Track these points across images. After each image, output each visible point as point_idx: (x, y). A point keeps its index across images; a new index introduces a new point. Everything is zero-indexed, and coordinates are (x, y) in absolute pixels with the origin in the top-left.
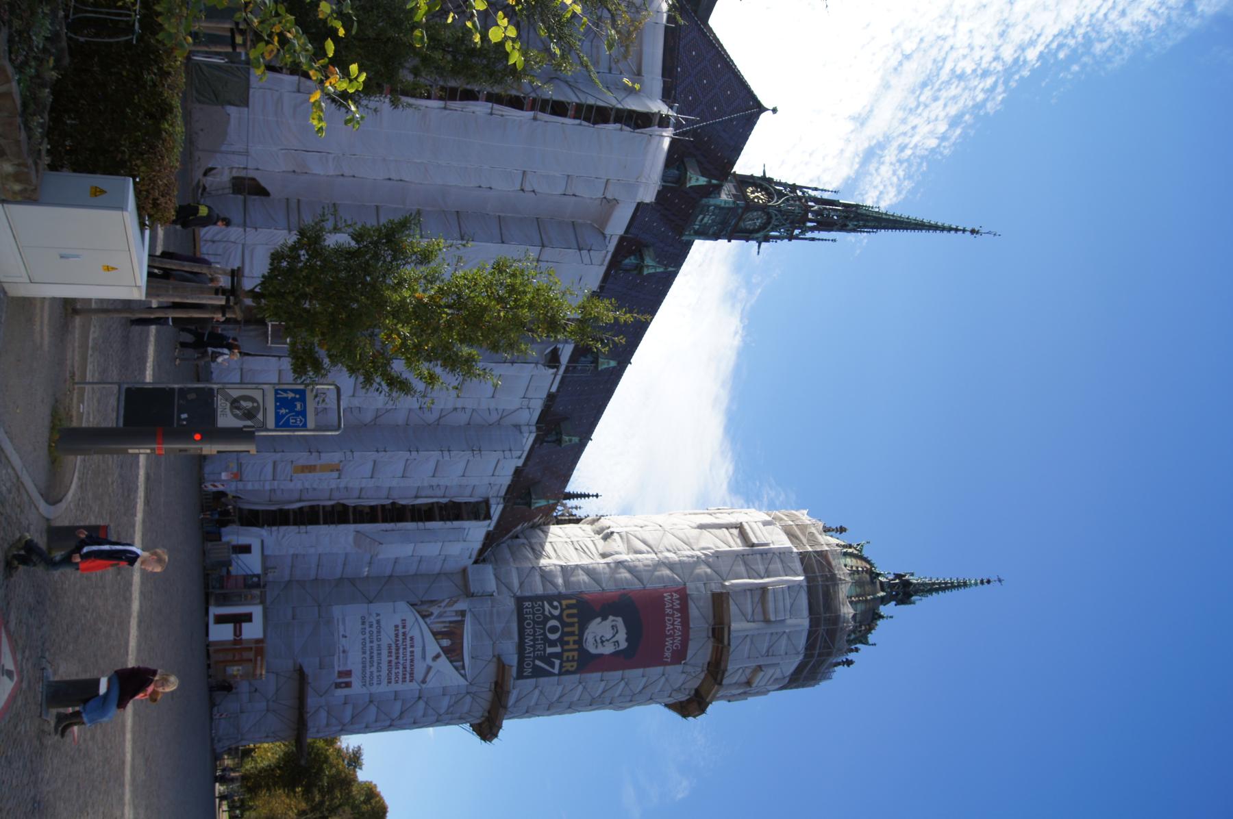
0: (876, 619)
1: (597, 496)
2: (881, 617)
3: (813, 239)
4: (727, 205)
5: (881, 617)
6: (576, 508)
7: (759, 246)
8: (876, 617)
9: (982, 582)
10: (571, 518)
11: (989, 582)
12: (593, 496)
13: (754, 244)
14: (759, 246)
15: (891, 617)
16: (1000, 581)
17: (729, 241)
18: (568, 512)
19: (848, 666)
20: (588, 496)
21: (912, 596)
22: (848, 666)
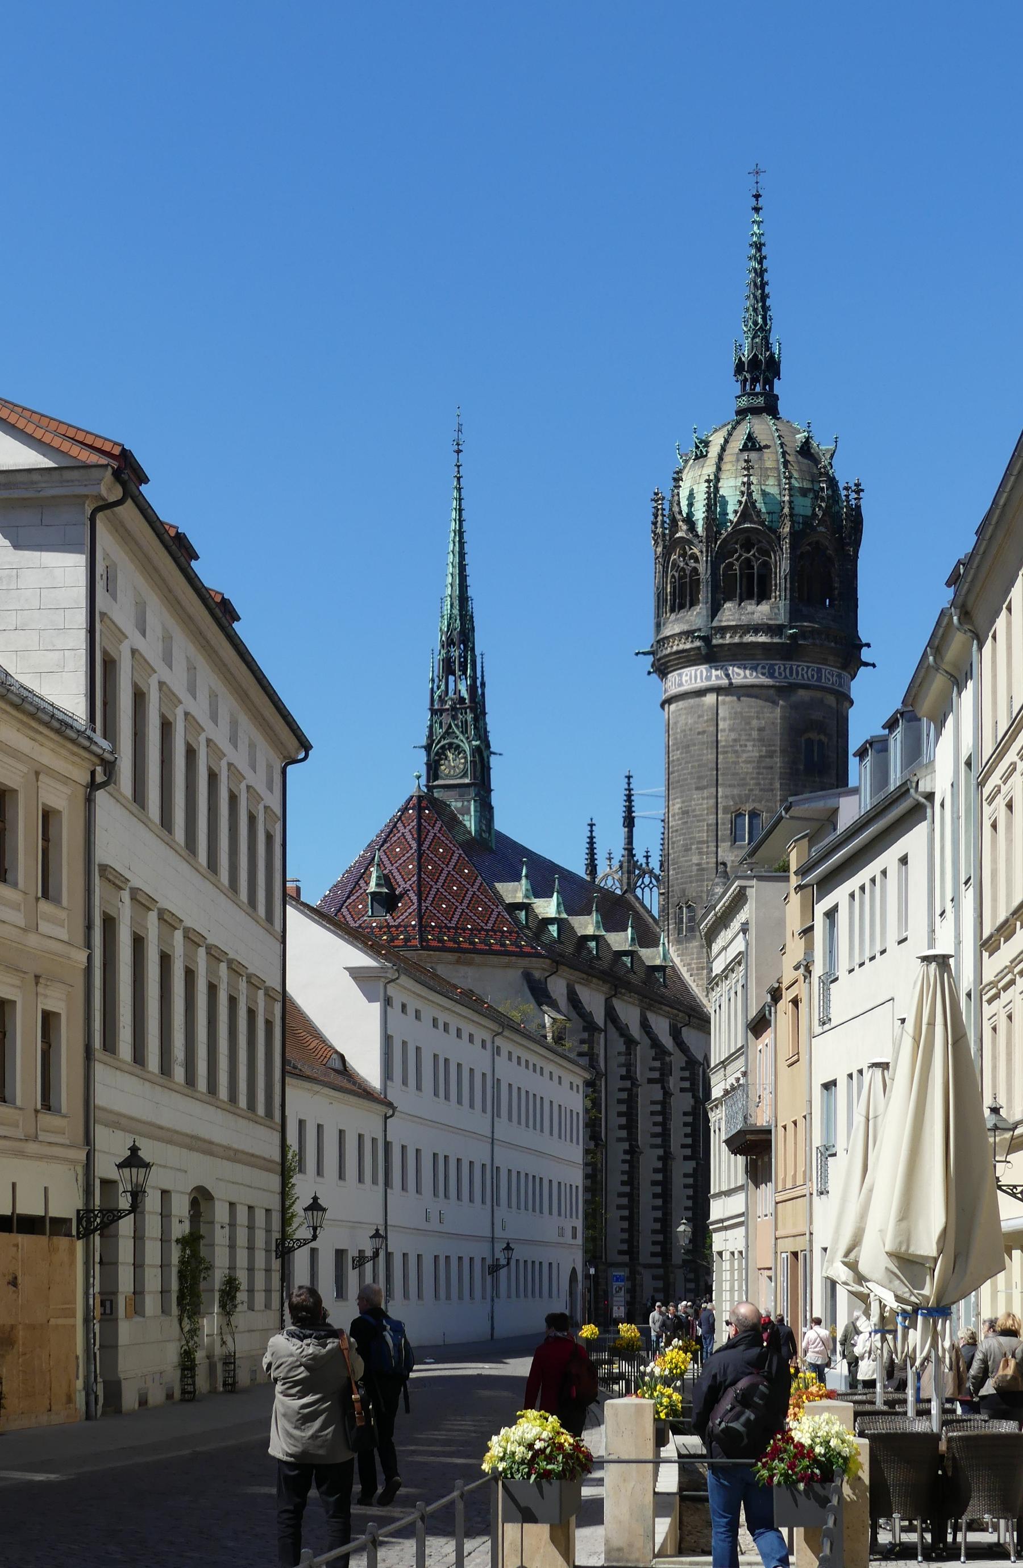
1: (591, 825)
3: (483, 684)
4: (479, 809)
5: (807, 443)
6: (610, 859)
7: (494, 753)
8: (806, 448)
9: (757, 210)
10: (625, 869)
11: (757, 197)
12: (591, 831)
13: (493, 758)
14: (494, 753)
17: (492, 790)
18: (616, 872)
20: (591, 838)
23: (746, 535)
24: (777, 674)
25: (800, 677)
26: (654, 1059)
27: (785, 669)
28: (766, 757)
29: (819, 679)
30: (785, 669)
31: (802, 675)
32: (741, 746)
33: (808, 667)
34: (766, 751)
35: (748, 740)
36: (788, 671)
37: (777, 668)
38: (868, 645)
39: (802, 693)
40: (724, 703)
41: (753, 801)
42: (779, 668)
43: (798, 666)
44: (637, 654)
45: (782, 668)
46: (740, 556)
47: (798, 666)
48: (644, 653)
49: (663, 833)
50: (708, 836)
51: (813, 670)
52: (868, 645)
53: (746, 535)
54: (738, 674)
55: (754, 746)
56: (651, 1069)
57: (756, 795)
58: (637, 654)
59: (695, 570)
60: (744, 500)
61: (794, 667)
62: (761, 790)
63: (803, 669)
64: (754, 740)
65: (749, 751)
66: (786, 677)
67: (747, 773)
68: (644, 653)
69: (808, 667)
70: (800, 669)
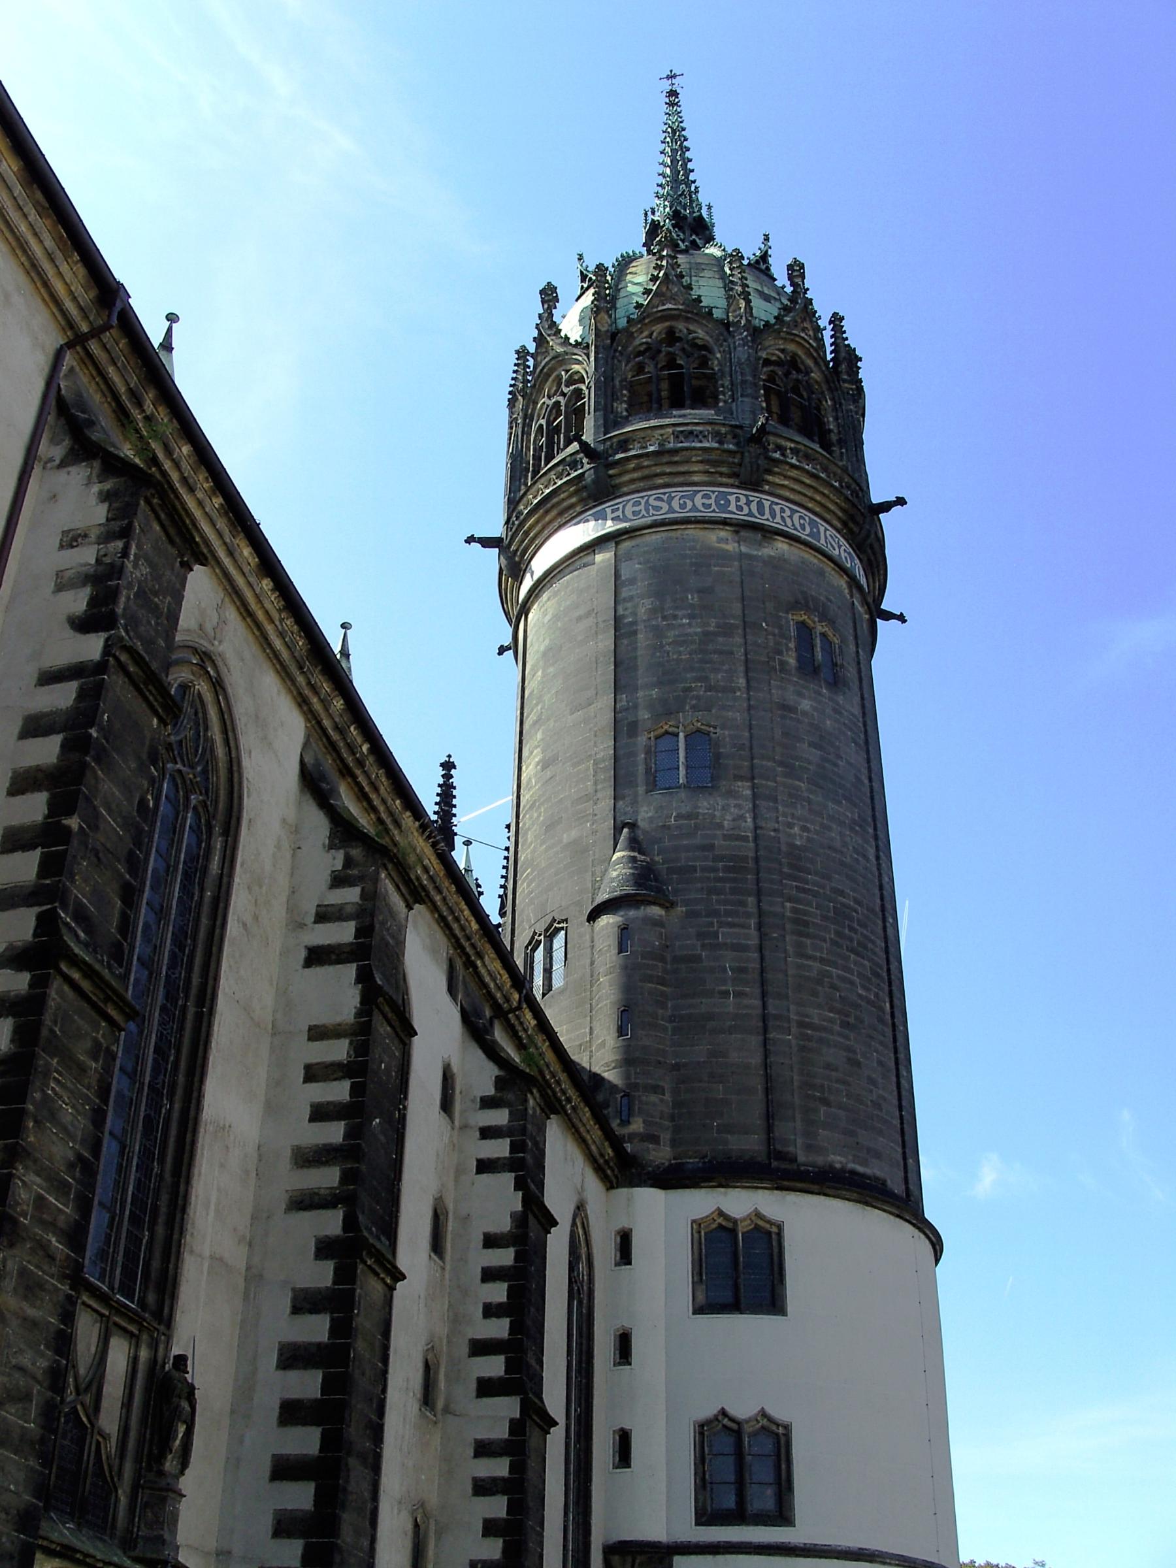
0: (768, 269)
2: (764, 257)
8: (763, 267)
15: (767, 238)
16: (672, 76)
19: (860, 359)
21: (701, 217)
22: (860, 359)
23: (667, 324)
24: (732, 508)
25: (778, 519)
26: (338, 881)
27: (748, 503)
28: (715, 634)
29: (816, 536)
30: (748, 503)
31: (782, 517)
32: (664, 618)
33: (793, 511)
34: (718, 626)
35: (677, 608)
36: (754, 507)
37: (732, 498)
38: (901, 501)
39: (781, 546)
40: (629, 557)
41: (695, 708)
42: (738, 499)
43: (777, 504)
44: (470, 540)
45: (743, 500)
46: (659, 351)
47: (777, 504)
48: (486, 542)
49: (507, 849)
50: (596, 783)
51: (801, 517)
52: (901, 501)
53: (667, 324)
54: (658, 508)
55: (691, 617)
56: (324, 915)
57: (698, 698)
58: (470, 540)
59: (578, 394)
60: (661, 275)
61: (767, 504)
62: (709, 688)
63: (782, 510)
64: (692, 606)
65: (684, 625)
66: (750, 514)
67: (678, 661)
68: (486, 542)
69: (793, 511)
70: (777, 508)
